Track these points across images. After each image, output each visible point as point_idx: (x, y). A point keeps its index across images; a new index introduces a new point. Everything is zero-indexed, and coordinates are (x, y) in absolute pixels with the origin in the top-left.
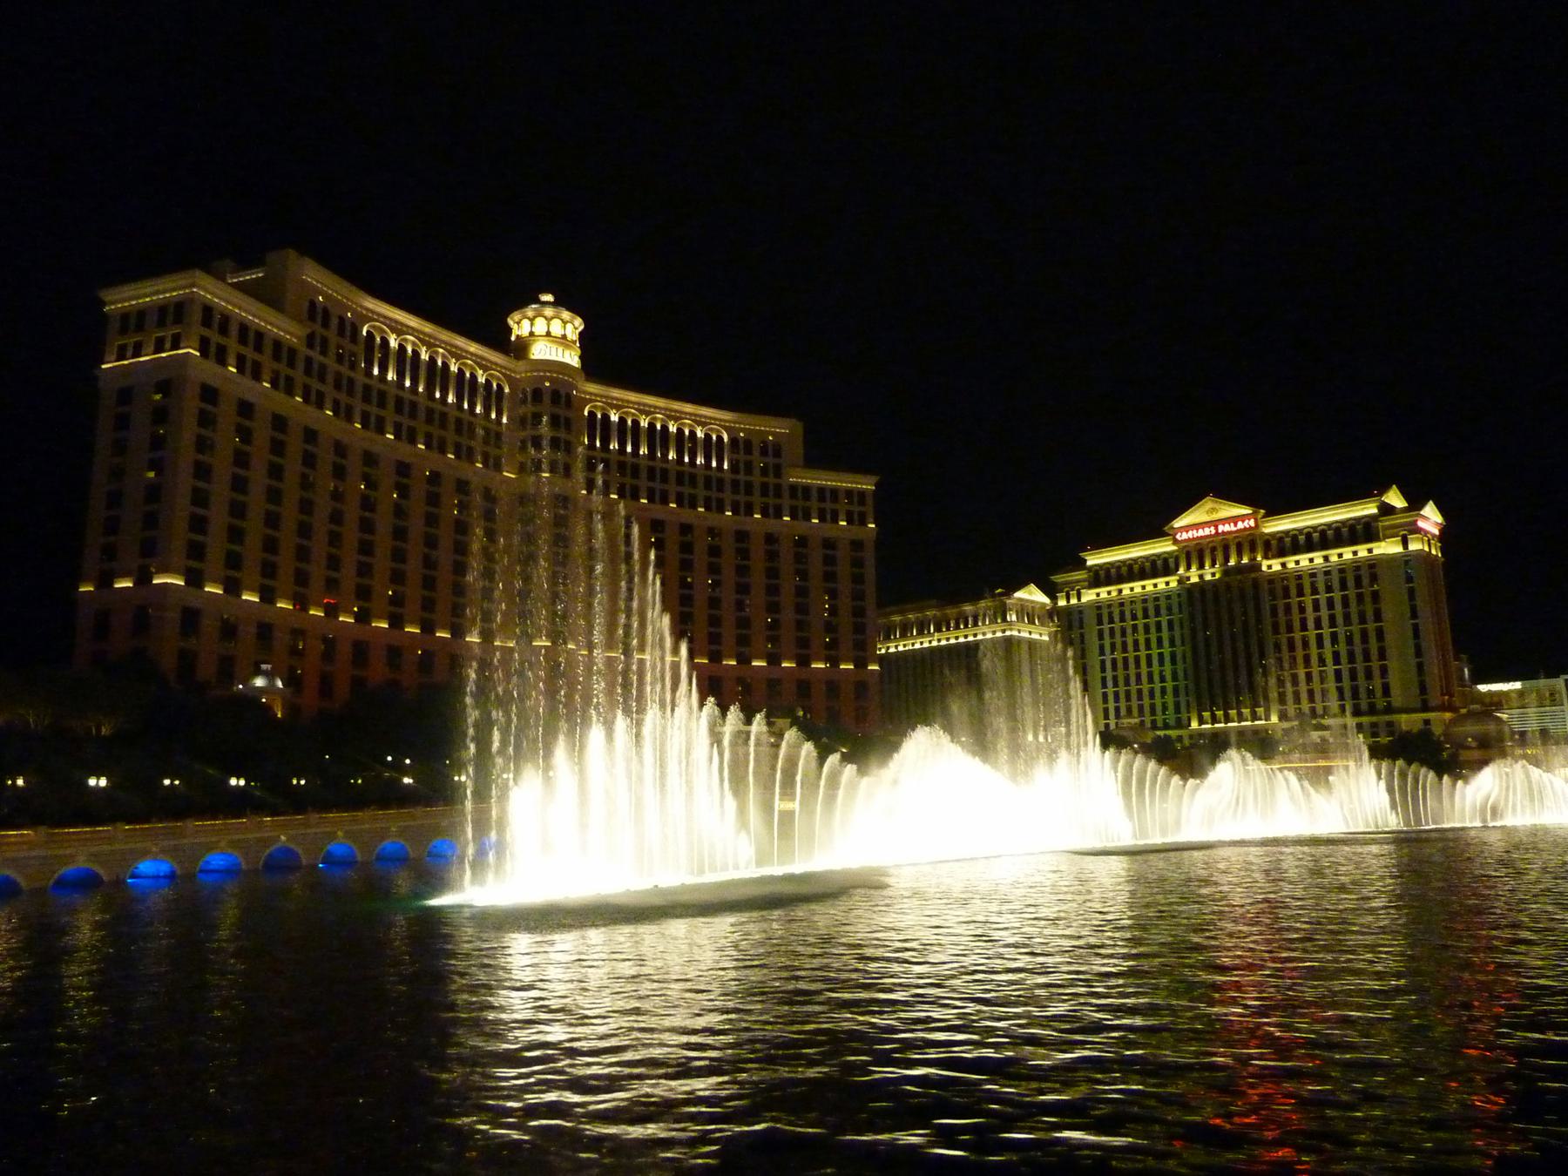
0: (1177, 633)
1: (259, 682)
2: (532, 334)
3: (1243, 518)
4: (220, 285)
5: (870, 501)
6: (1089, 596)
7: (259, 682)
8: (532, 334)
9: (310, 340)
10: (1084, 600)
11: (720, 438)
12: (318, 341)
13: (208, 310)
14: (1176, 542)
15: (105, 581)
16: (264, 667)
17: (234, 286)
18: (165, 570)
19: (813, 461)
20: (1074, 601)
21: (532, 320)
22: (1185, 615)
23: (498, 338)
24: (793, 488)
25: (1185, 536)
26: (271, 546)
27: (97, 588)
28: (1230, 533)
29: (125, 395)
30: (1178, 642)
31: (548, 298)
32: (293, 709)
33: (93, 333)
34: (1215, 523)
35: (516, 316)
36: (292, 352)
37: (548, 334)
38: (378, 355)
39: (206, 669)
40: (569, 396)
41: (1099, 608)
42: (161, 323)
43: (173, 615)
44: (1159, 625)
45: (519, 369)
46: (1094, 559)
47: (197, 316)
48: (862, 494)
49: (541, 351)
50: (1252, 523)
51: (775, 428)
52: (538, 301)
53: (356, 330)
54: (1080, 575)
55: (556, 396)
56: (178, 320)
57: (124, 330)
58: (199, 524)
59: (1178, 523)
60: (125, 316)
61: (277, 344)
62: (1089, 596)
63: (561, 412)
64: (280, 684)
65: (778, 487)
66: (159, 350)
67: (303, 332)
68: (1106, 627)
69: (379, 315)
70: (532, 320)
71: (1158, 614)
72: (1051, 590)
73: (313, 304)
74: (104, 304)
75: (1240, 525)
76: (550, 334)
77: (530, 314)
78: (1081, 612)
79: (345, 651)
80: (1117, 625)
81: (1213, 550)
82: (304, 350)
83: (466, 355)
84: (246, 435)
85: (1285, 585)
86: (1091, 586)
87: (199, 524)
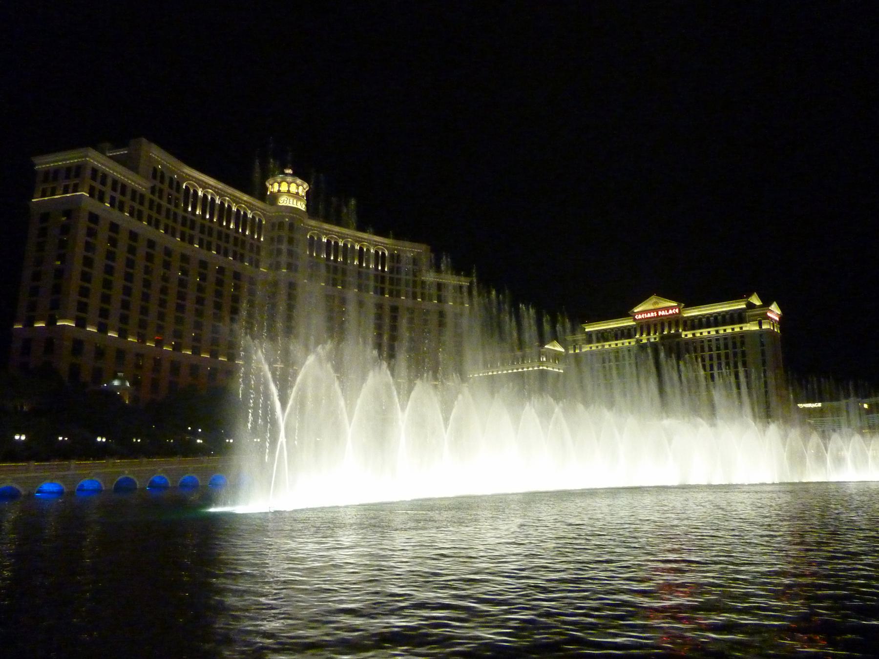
1: (116, 383)
2: (279, 191)
7: (116, 383)
8: (279, 191)
9: (153, 190)
13: (95, 171)
15: (29, 322)
16: (119, 374)
17: (110, 157)
18: (64, 318)
21: (280, 184)
26: (125, 305)
27: (25, 326)
29: (45, 217)
32: (135, 399)
33: (28, 182)
35: (271, 181)
36: (142, 196)
37: (289, 191)
38: (191, 200)
39: (86, 376)
42: (67, 177)
43: (68, 344)
47: (88, 173)
49: (284, 201)
52: (283, 173)
53: (179, 185)
56: (77, 175)
58: (84, 292)
60: (47, 173)
61: (134, 192)
64: (128, 384)
67: (149, 185)
69: (193, 177)
70: (280, 184)
73: (155, 170)
76: (290, 192)
77: (279, 180)
79: (166, 366)
82: (149, 195)
83: (238, 200)
84: (113, 242)
87: (84, 292)
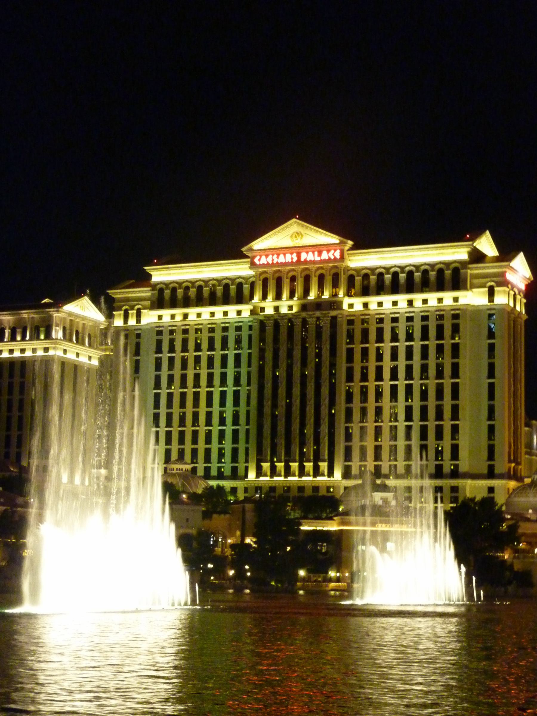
0: (244, 370)
6: (150, 317)
10: (145, 321)
14: (253, 265)
20: (132, 322)
22: (255, 351)
25: (264, 261)
28: (313, 262)
30: (244, 380)
34: (298, 250)
41: (160, 333)
44: (224, 358)
46: (161, 275)
54: (144, 292)
59: (258, 244)
62: (150, 317)
71: (225, 345)
78: (138, 336)
80: (178, 355)
81: (293, 279)
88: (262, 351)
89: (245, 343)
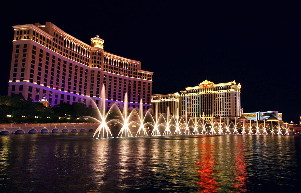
2: (95, 42)
3: (211, 84)
4: (36, 27)
5: (151, 76)
8: (95, 42)
9: (54, 39)
11: (127, 64)
12: (55, 40)
13: (34, 32)
17: (39, 28)
19: (143, 69)
21: (95, 40)
23: (89, 43)
24: (139, 73)
31: (98, 36)
33: (12, 34)
35: (92, 39)
36: (50, 41)
37: (98, 43)
40: (101, 54)
44: (196, 100)
45: (93, 49)
48: (150, 75)
49: (97, 46)
50: (212, 85)
51: (137, 63)
54: (185, 91)
55: (99, 54)
56: (28, 33)
57: (18, 34)
59: (201, 84)
60: (18, 32)
61: (48, 40)
62: (186, 95)
63: (100, 57)
65: (136, 73)
66: (25, 38)
68: (188, 100)
69: (67, 36)
72: (180, 93)
73: (55, 33)
74: (14, 29)
75: (210, 85)
76: (98, 43)
77: (95, 39)
82: (53, 41)
85: (215, 95)
86: (186, 93)
88: (202, 99)
89: (199, 98)
